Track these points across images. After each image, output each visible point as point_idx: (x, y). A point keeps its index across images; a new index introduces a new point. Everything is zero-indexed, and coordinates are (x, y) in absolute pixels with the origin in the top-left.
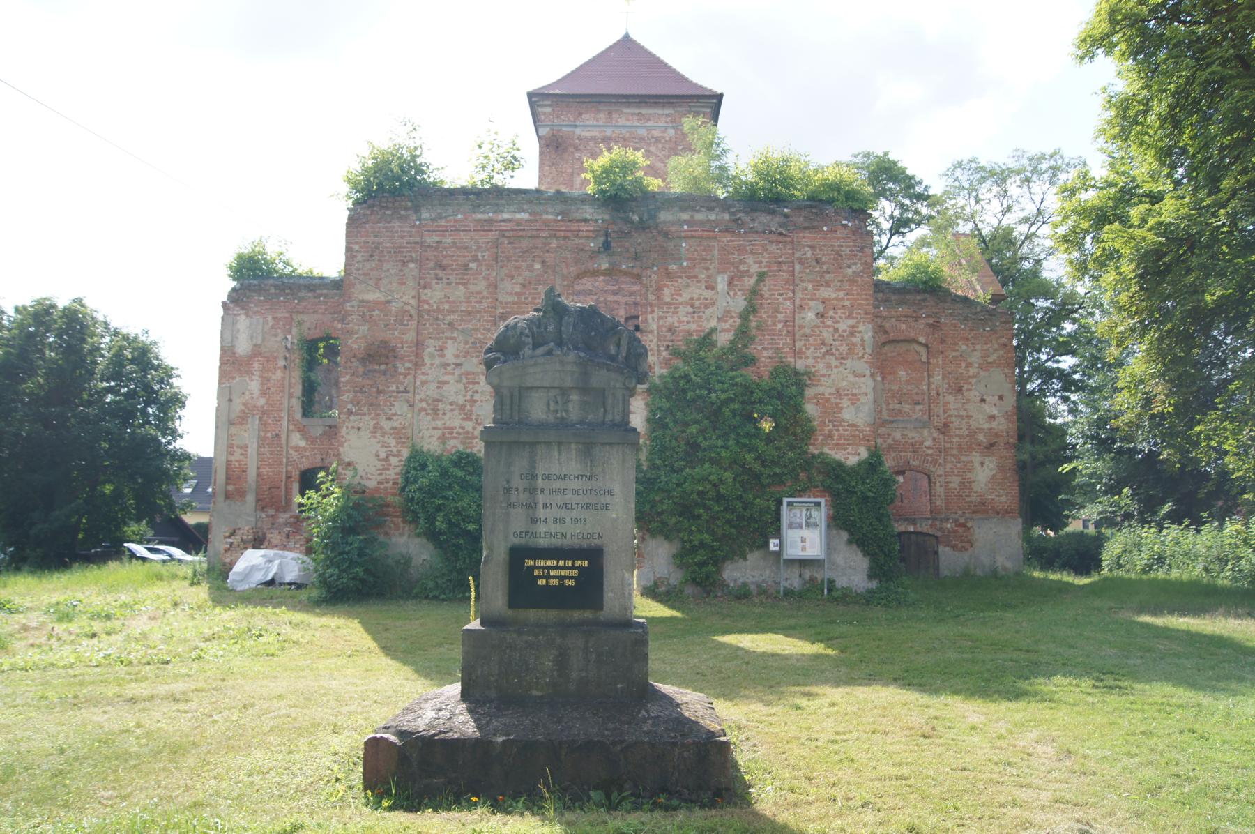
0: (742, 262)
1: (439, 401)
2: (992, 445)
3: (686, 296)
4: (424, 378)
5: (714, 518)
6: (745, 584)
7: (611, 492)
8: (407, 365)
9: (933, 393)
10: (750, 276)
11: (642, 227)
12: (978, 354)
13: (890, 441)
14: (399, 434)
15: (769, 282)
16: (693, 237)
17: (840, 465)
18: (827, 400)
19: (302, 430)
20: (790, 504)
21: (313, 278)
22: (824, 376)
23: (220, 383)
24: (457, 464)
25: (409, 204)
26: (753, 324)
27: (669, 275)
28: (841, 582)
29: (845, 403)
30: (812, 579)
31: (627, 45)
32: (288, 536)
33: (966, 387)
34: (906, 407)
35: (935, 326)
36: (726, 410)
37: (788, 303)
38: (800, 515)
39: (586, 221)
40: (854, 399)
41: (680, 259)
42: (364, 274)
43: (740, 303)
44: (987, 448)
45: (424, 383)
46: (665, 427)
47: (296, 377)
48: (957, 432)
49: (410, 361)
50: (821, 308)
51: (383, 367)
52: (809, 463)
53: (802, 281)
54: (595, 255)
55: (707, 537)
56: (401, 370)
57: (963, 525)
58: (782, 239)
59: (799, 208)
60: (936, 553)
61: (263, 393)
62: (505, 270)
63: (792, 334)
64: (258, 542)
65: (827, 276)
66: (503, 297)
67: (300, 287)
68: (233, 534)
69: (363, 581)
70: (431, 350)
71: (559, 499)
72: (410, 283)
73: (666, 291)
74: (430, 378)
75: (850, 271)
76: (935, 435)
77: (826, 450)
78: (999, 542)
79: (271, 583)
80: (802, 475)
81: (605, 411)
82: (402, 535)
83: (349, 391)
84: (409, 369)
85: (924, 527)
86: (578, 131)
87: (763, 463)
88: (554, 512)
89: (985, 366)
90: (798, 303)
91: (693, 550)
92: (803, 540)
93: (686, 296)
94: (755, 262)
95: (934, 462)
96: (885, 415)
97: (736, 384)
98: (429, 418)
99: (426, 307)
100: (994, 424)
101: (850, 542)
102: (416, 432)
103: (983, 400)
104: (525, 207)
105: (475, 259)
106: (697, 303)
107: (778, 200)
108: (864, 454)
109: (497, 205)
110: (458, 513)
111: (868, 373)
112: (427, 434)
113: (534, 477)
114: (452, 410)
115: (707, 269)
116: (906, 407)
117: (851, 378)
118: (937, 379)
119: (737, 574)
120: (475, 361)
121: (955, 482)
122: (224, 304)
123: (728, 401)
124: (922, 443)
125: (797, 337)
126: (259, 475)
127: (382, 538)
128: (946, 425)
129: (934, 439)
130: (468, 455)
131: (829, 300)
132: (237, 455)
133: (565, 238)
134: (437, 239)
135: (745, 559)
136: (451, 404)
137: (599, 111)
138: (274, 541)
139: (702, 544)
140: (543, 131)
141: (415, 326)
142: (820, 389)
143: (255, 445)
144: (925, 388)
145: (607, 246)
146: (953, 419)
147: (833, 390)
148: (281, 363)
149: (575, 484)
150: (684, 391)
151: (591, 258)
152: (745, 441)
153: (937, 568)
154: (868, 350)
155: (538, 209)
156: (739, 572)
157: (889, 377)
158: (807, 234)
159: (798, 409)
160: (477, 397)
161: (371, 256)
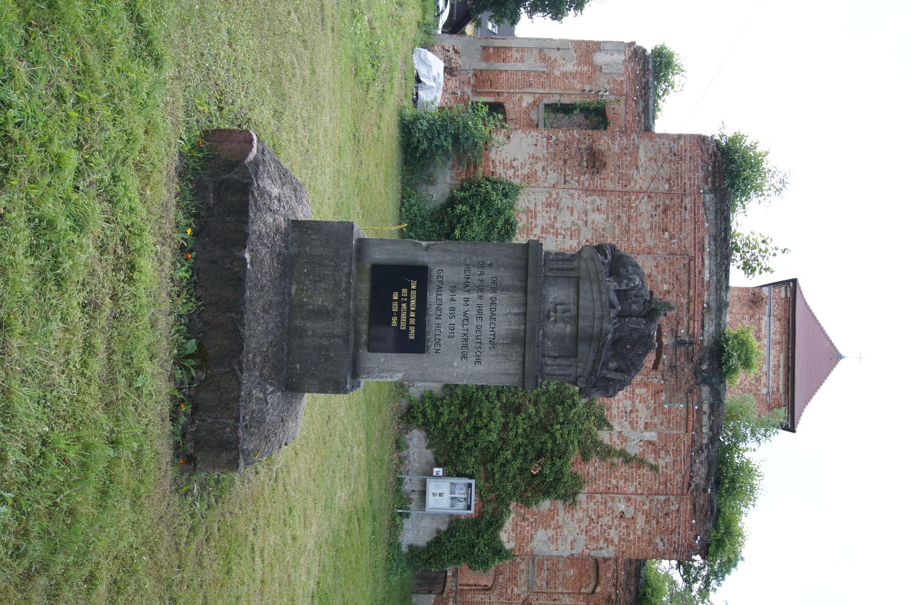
0: (667, 452)
1: (558, 207)
3: (639, 406)
4: (576, 196)
5: (460, 424)
6: (407, 447)
7: (478, 361)
8: (586, 184)
9: (556, 596)
10: (655, 459)
11: (696, 372)
14: (530, 177)
15: (650, 474)
16: (688, 413)
17: (500, 526)
18: (553, 518)
19: (535, 104)
20: (470, 485)
21: (654, 112)
22: (573, 515)
23: (572, 41)
24: (507, 221)
25: (717, 185)
26: (615, 460)
27: (657, 393)
28: (407, 523)
29: (550, 532)
30: (410, 501)
32: (453, 93)
34: (544, 574)
37: (633, 489)
38: (461, 493)
39: (703, 327)
40: (553, 540)
41: (670, 402)
42: (660, 148)
43: (633, 450)
45: (572, 196)
47: (577, 100)
49: (589, 185)
50: (628, 515)
51: (585, 164)
52: (502, 501)
53: (651, 501)
54: (674, 333)
55: (445, 418)
56: (582, 178)
59: (711, 501)
60: (430, 592)
61: (564, 74)
62: (662, 261)
63: (607, 491)
64: (449, 71)
65: (654, 522)
67: (646, 101)
68: (456, 52)
69: (417, 148)
70: (598, 202)
71: (473, 312)
73: (644, 391)
74: (576, 200)
75: (658, 540)
76: (522, 596)
77: (513, 515)
79: (418, 80)
80: (492, 496)
81: (555, 358)
82: (452, 178)
83: (566, 137)
84: (583, 184)
85: (450, 584)
86: (766, 318)
88: (460, 308)
90: (633, 497)
91: (436, 407)
92: (441, 495)
93: (639, 406)
94: (667, 463)
97: (567, 445)
98: (544, 200)
99: (633, 198)
101: (438, 531)
102: (533, 190)
104: (714, 278)
105: (672, 237)
106: (633, 415)
107: (718, 483)
108: (508, 546)
109: (716, 255)
110: (468, 222)
111: (574, 552)
112: (532, 198)
113: (494, 290)
114: (550, 218)
115: (662, 424)
116: (544, 574)
117: (570, 538)
119: (415, 441)
120: (589, 237)
122: (633, 43)
124: (516, 585)
125: (605, 495)
126: (501, 71)
127: (450, 163)
129: (519, 595)
130: (513, 230)
131: (635, 523)
132: (516, 55)
133: (688, 309)
134: (688, 207)
135: (428, 448)
136: (555, 218)
137: (782, 334)
138: (450, 84)
139: (440, 414)
140: (765, 291)
141: (617, 189)
142: (562, 512)
143: (523, 68)
144: (560, 590)
145: (679, 343)
147: (560, 523)
148: (587, 88)
149: (486, 329)
150: (562, 403)
151: (672, 330)
152: (521, 451)
154: (592, 553)
155: (712, 288)
156: (416, 439)
157: (569, 562)
158: (689, 507)
159: (546, 494)
160: (560, 238)
161: (675, 155)
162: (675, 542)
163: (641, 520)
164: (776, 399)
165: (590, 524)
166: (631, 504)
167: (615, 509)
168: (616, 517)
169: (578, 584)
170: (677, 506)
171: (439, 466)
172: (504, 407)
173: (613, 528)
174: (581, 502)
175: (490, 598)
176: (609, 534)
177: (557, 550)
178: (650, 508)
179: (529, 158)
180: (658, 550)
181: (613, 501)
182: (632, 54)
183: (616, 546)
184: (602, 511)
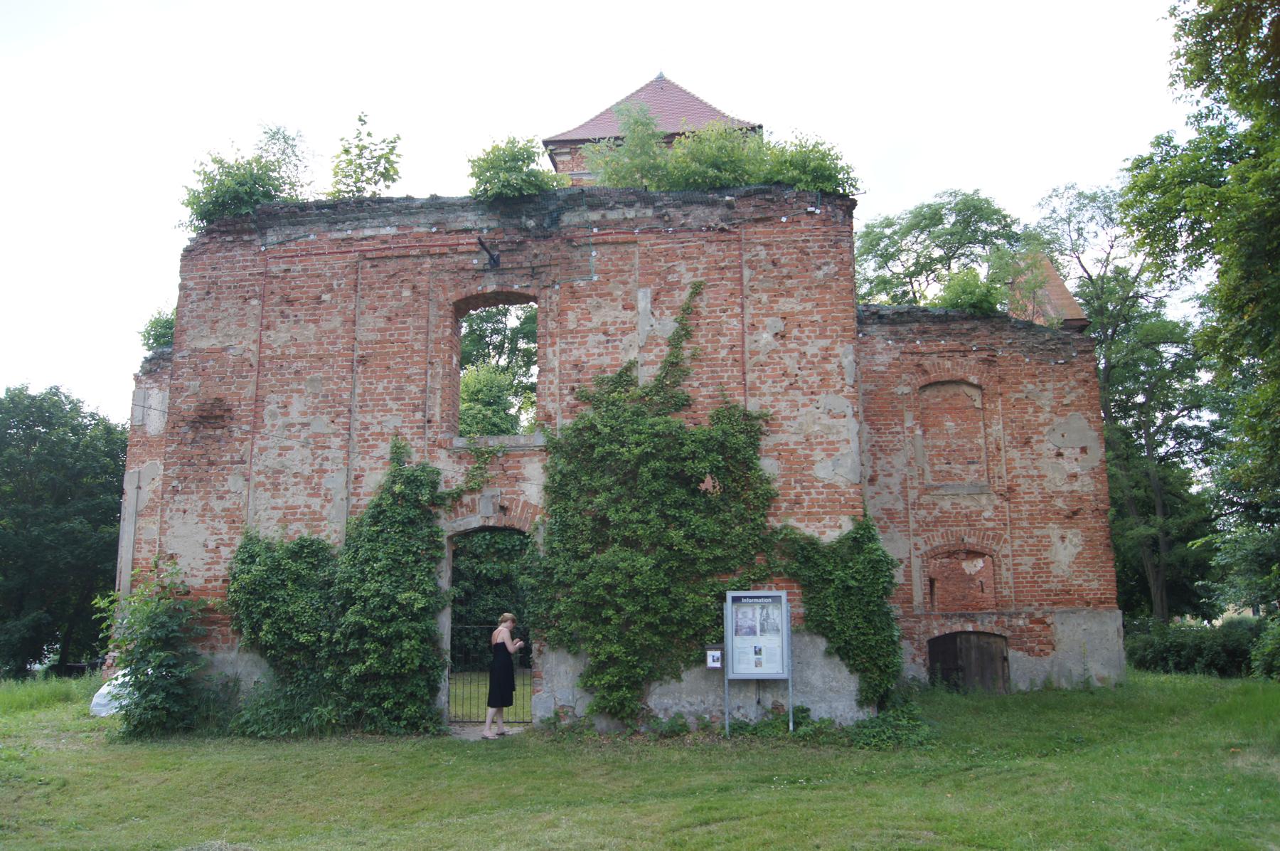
0: (670, 270)
1: (279, 472)
2: (1075, 513)
3: (596, 320)
4: (262, 443)
5: (629, 622)
6: (679, 715)
9: (992, 447)
10: (682, 289)
12: (1049, 394)
13: (936, 513)
14: (233, 519)
15: (707, 295)
16: (605, 243)
17: (812, 543)
22: (784, 418)
24: (295, 554)
25: (253, 226)
26: (687, 353)
27: (574, 294)
28: (819, 711)
29: (818, 454)
31: (661, 85)
33: (1035, 437)
34: (957, 468)
35: (990, 362)
36: (643, 469)
37: (734, 322)
38: (750, 614)
39: (467, 231)
40: (831, 449)
41: (589, 272)
42: (198, 317)
43: (668, 325)
44: (1068, 517)
46: (567, 496)
48: (1027, 498)
49: (247, 423)
50: (780, 326)
51: (219, 432)
52: (766, 542)
54: (479, 273)
55: (616, 649)
56: (237, 434)
57: (1040, 621)
58: (724, 237)
59: (748, 195)
60: (1005, 659)
62: (367, 301)
63: (740, 363)
65: (789, 283)
66: (362, 335)
70: (273, 407)
72: (252, 324)
73: (571, 316)
74: (269, 443)
75: (820, 274)
76: (997, 502)
77: (792, 522)
78: (1092, 643)
80: (759, 560)
82: (231, 649)
83: (175, 464)
84: (247, 432)
87: (700, 542)
89: (1061, 409)
90: (748, 320)
91: (600, 668)
93: (596, 320)
94: (689, 270)
95: (997, 538)
97: (657, 435)
98: (269, 494)
99: (268, 352)
100: (1076, 486)
101: (828, 653)
103: (1059, 455)
104: (392, 219)
105: (330, 289)
106: (612, 329)
107: (723, 188)
108: (847, 526)
109: (358, 219)
110: (290, 620)
111: (849, 412)
112: (264, 515)
114: (296, 484)
115: (625, 283)
116: (957, 468)
117: (826, 420)
118: (997, 429)
119: (667, 701)
121: (1027, 563)
122: (136, 377)
123: (645, 458)
124: (979, 513)
125: (748, 367)
127: (206, 654)
129: (996, 508)
130: (312, 543)
131: (792, 315)
133: (441, 255)
134: (284, 267)
135: (679, 678)
136: (295, 475)
139: (612, 660)
141: (255, 378)
142: (781, 438)
144: (981, 441)
145: (494, 263)
146: (1020, 481)
147: (801, 438)
150: (592, 447)
151: (475, 278)
152: (671, 512)
153: (1007, 679)
154: (849, 381)
155: (407, 221)
156: (667, 700)
157: (932, 430)
158: (760, 228)
159: (748, 465)
160: (327, 465)
161: (208, 293)
162: (822, 247)
163: (786, 305)
165: (799, 388)
166: (761, 322)
167: (770, 348)
168: (784, 345)
169: (969, 412)
170: (759, 248)
171: (703, 660)
172: (602, 545)
173: (803, 349)
174: (762, 407)
175: (1006, 556)
176: (815, 356)
178: (765, 291)
179: (203, 522)
180: (836, 273)
181: (758, 353)
182: (150, 378)
183: (834, 343)
184: (774, 370)
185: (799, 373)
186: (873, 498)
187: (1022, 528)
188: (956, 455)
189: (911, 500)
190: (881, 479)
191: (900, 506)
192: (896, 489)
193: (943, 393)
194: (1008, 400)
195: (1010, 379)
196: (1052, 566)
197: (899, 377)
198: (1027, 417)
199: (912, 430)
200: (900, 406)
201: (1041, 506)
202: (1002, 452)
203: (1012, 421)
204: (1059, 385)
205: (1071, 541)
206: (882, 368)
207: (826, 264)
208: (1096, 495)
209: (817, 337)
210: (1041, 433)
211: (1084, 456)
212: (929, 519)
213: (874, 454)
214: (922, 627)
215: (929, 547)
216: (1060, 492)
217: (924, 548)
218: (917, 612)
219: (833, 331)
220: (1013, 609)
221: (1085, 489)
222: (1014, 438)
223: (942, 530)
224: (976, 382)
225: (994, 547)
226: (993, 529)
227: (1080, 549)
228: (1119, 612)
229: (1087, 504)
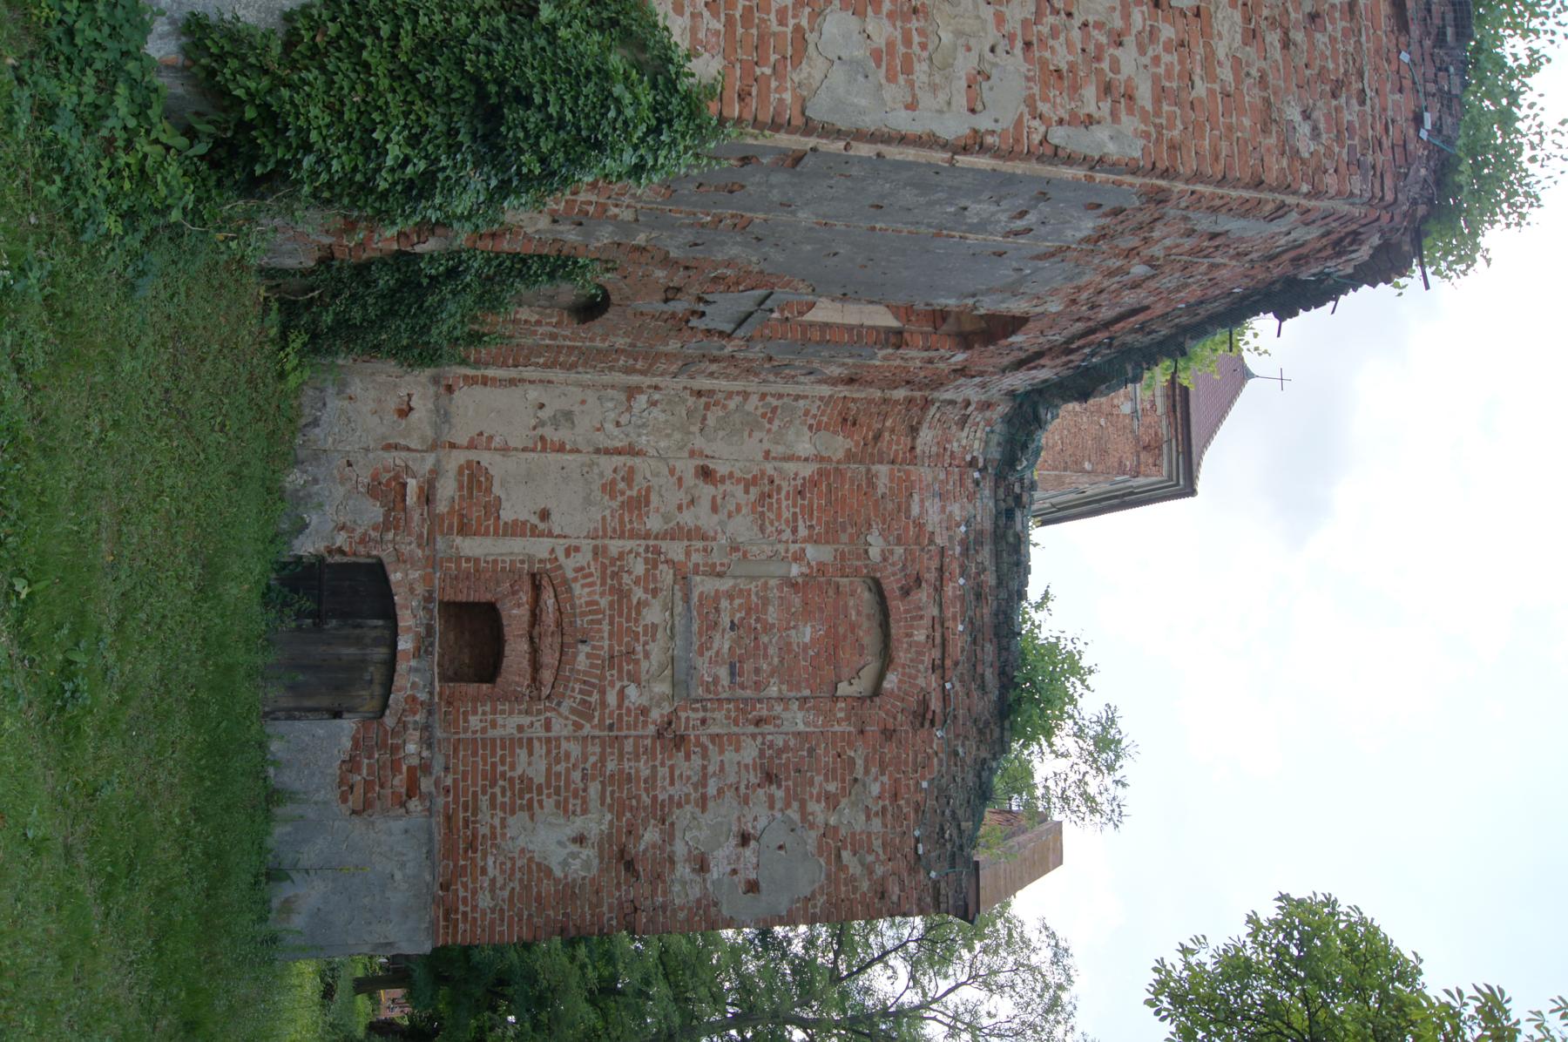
2: (630, 866)
12: (860, 824)
13: (639, 594)
29: (881, 30)
33: (779, 794)
34: (723, 642)
35: (922, 716)
40: (893, 62)
44: (622, 852)
48: (663, 772)
57: (412, 789)
60: (337, 715)
65: (1273, 38)
75: (1294, 114)
76: (655, 714)
89: (833, 844)
96: (704, 586)
100: (683, 870)
103: (745, 839)
111: (983, 122)
116: (723, 642)
117: (965, 65)
118: (797, 720)
121: (533, 766)
124: (634, 678)
128: (680, 741)
129: (644, 711)
131: (1206, 33)
144: (773, 691)
146: (697, 761)
153: (290, 715)
157: (797, 600)
164: (1150, 426)
165: (1039, 14)
173: (1130, 41)
175: (548, 726)
177: (911, 106)
183: (1145, 120)
185: (1077, 22)
186: (672, 472)
187: (603, 759)
188: (748, 641)
189: (664, 545)
190: (707, 491)
191: (654, 523)
192: (687, 518)
193: (866, 624)
194: (851, 744)
195: (889, 750)
196: (525, 815)
197: (899, 541)
198: (818, 779)
199: (799, 557)
200: (844, 538)
201: (646, 800)
202: (751, 729)
203: (811, 751)
204: (877, 843)
205: (574, 855)
206: (915, 510)
207: (1316, 133)
208: (664, 907)
209: (1156, 79)
210: (788, 805)
211: (742, 888)
212: (626, 579)
213: (754, 481)
214: (410, 547)
215: (570, 574)
216: (672, 837)
217: (569, 565)
218: (440, 543)
219: (1171, 118)
220: (439, 734)
221: (677, 888)
222: (780, 752)
223: (604, 603)
224: (886, 685)
225: (567, 704)
226: (603, 704)
227: (559, 873)
228: (427, 948)
229: (646, 889)
